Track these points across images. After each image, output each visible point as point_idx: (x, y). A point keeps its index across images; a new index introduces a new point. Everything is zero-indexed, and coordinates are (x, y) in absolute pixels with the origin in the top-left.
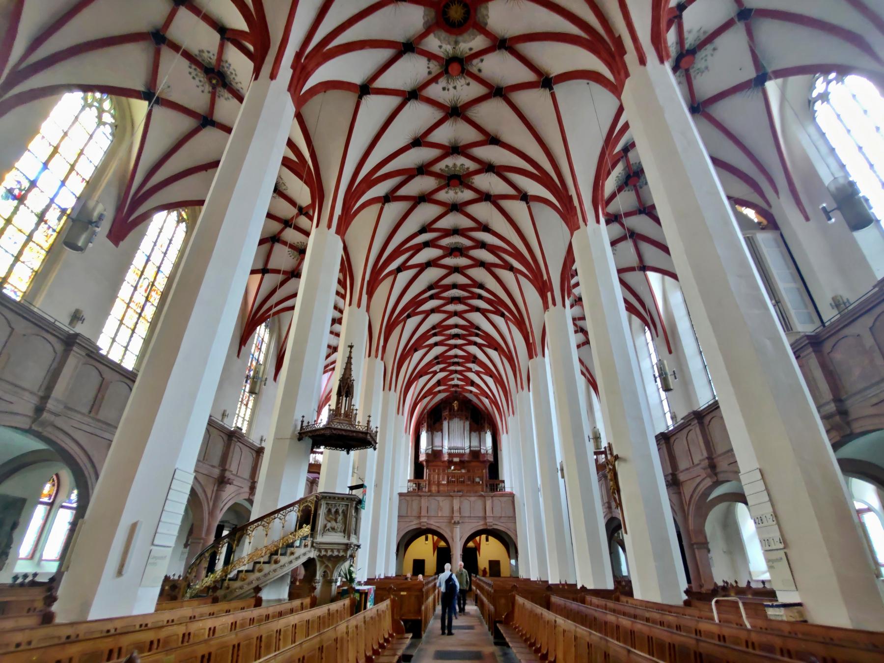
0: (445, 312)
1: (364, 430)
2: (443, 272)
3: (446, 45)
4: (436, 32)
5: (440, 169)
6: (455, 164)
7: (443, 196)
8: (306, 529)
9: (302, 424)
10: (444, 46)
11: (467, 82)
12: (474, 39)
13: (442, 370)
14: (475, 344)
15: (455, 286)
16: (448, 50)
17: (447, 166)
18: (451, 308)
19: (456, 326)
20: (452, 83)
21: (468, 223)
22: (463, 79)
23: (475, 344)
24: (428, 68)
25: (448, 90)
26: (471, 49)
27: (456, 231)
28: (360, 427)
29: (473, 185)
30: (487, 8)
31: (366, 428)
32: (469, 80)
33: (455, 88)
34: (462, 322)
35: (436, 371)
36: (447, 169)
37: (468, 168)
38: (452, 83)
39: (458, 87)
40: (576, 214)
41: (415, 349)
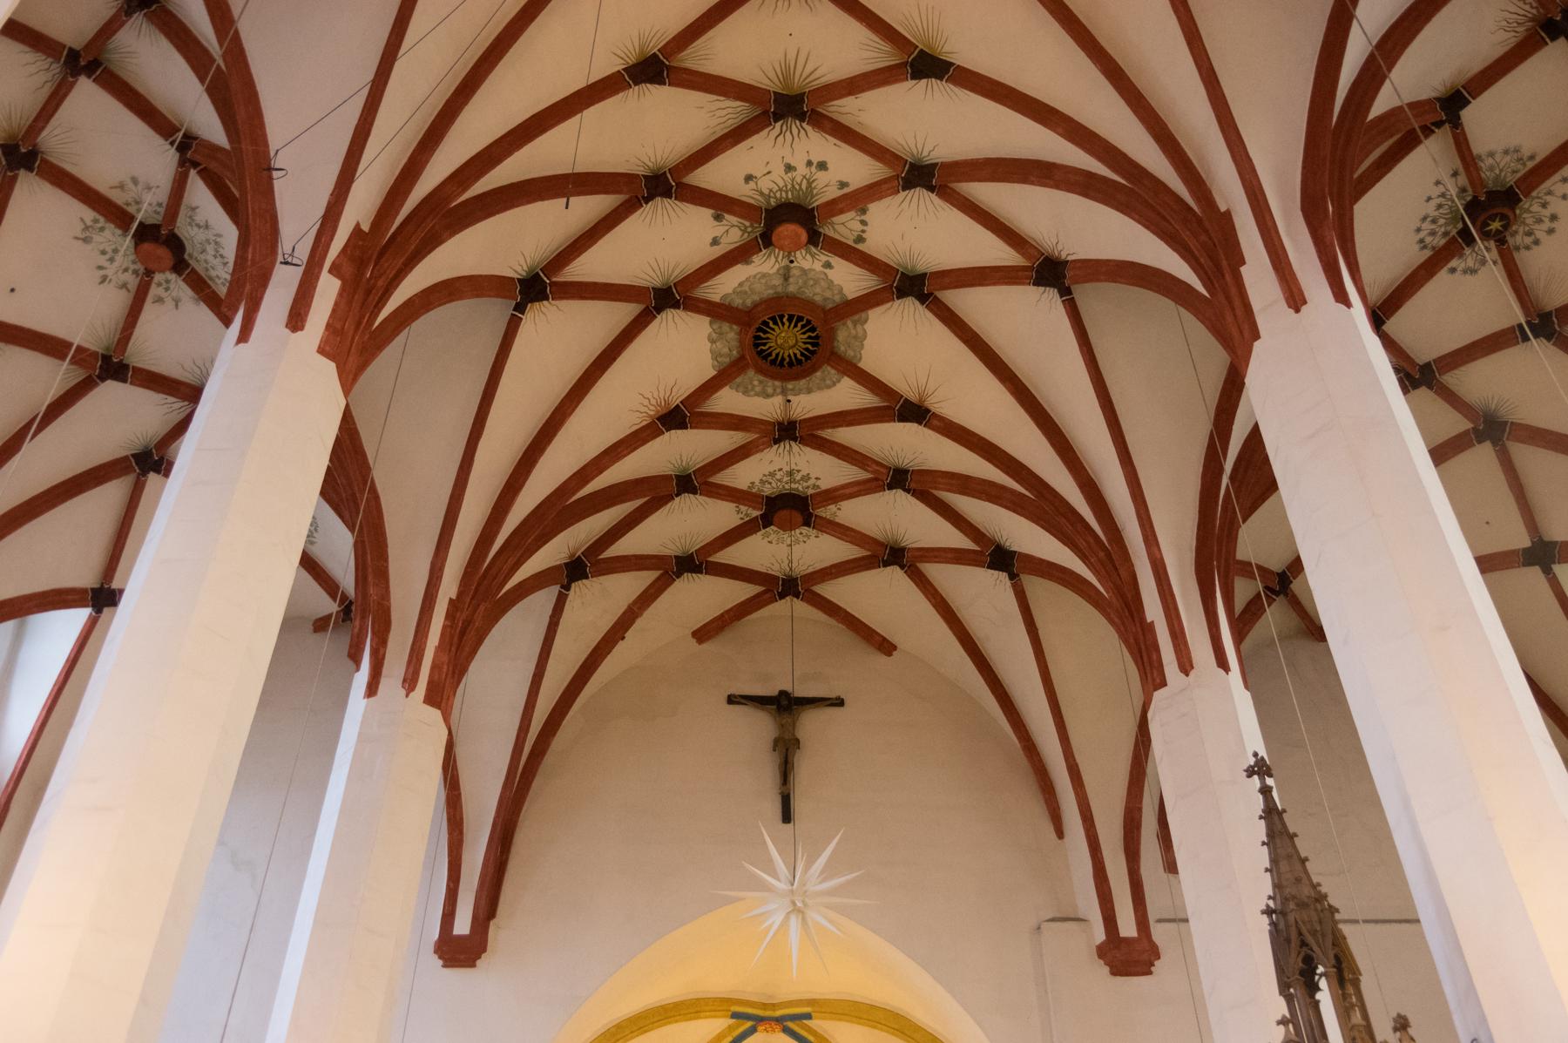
4: (837, 298)
10: (818, 266)
11: (752, 184)
12: (741, 285)
16: (808, 257)
20: (798, 179)
22: (767, 192)
24: (864, 223)
25: (809, 163)
30: (715, 355)
33: (789, 168)
38: (798, 179)
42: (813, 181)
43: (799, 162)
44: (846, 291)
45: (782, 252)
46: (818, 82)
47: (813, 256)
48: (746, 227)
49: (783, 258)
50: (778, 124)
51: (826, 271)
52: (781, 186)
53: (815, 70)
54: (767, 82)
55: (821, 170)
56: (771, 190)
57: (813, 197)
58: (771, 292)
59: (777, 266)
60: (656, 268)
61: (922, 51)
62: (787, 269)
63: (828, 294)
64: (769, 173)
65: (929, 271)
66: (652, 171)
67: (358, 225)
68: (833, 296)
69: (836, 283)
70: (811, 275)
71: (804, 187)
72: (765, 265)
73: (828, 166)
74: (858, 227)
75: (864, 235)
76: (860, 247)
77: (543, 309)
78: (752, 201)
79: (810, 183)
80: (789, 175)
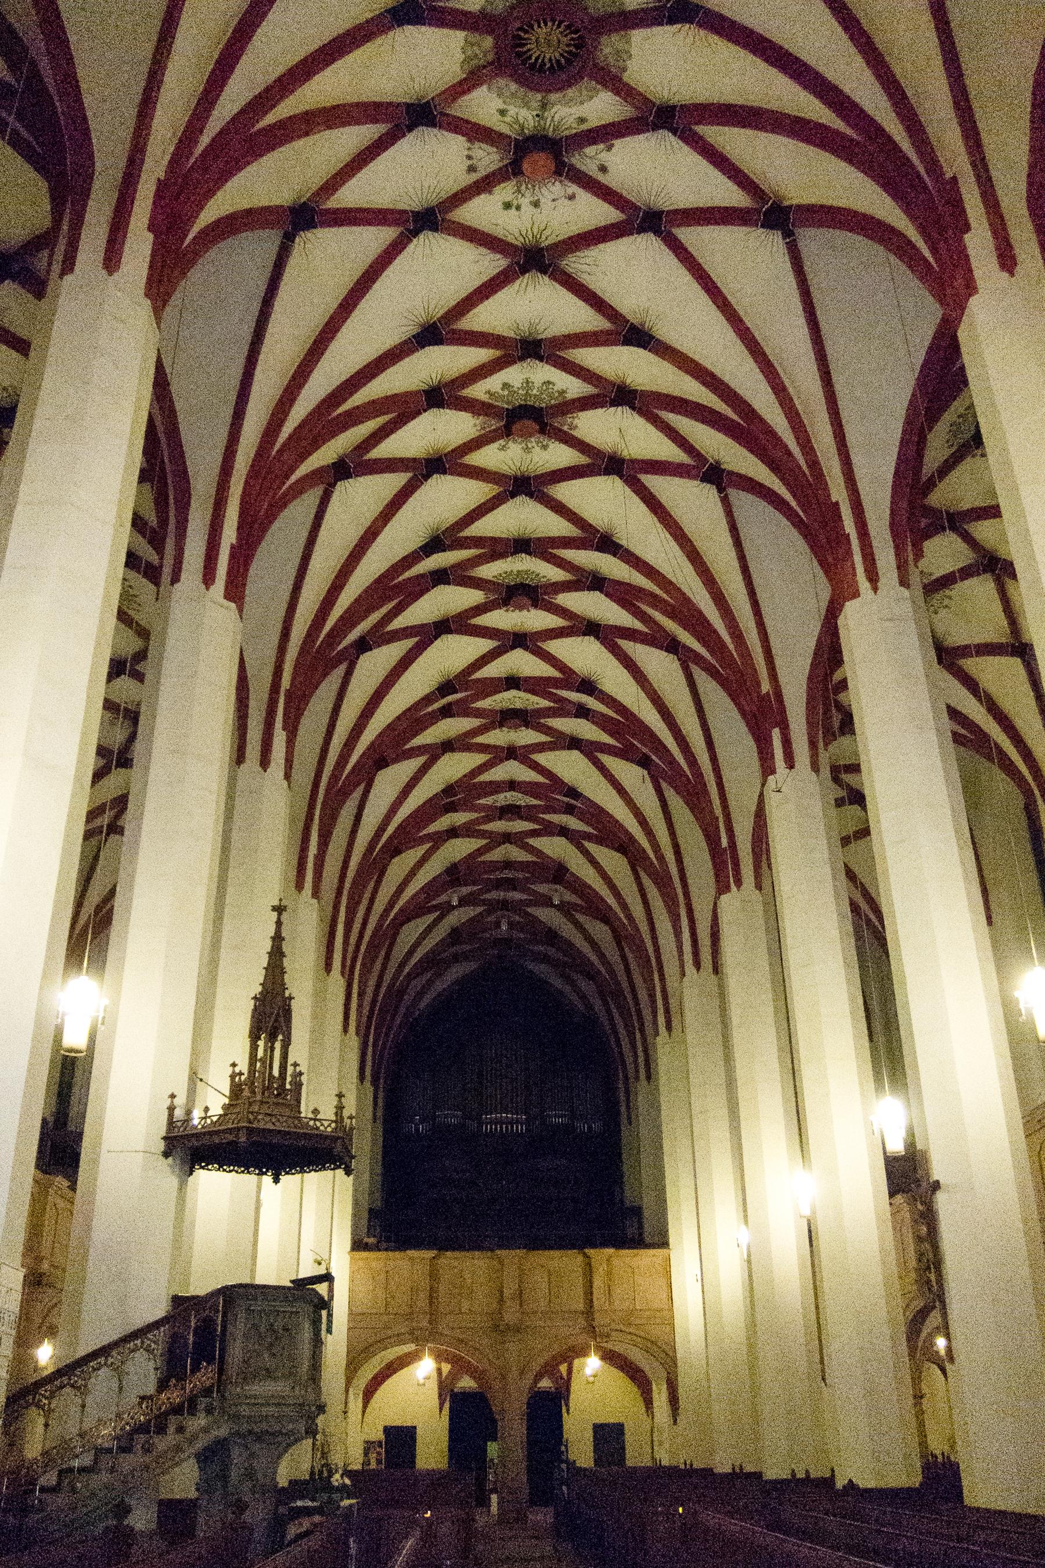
0: (483, 748)
1: (329, 1129)
2: (484, 645)
5: (488, 392)
7: (489, 457)
8: (206, 1376)
9: (171, 1115)
10: (512, 111)
12: (591, 98)
13: (463, 902)
14: (563, 831)
15: (512, 682)
17: (506, 386)
18: (498, 737)
19: (512, 785)
21: (558, 526)
23: (563, 831)
24: (469, 157)
25: (518, 208)
26: (582, 120)
27: (522, 545)
28: (318, 1124)
29: (575, 433)
31: (333, 1125)
32: (573, 188)
33: (536, 204)
34: (530, 776)
35: (449, 903)
38: (528, 194)
40: (849, 553)
41: (394, 849)
43: (527, 209)
64: (554, 200)
71: (523, 187)
79: (519, 191)
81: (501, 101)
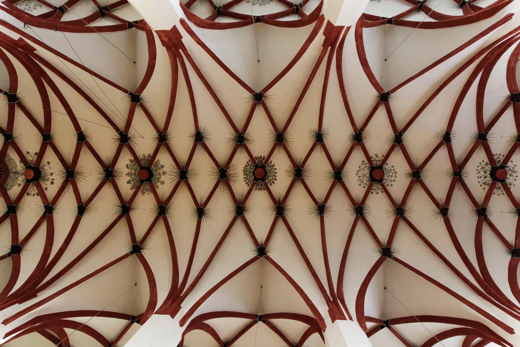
3: (18, 181)
4: (7, 188)
6: (128, 174)
10: (19, 182)
11: (47, 164)
12: (13, 160)
16: (22, 179)
17: (129, 182)
20: (48, 177)
22: (44, 168)
24: (34, 195)
25: (53, 180)
33: (52, 174)
36: (132, 182)
37: (131, 161)
38: (48, 177)
39: (51, 171)
42: (48, 181)
43: (53, 177)
44: (10, 190)
45: (24, 172)
46: (77, 182)
47: (22, 181)
48: (33, 162)
49: (22, 172)
50: (65, 171)
51: (18, 184)
52: (46, 172)
53: (81, 181)
54: (78, 168)
55: (51, 183)
56: (45, 169)
57: (42, 181)
58: (10, 168)
59: (19, 170)
60: (19, 135)
61: (86, 208)
62: (18, 173)
63: (9, 185)
64: (50, 168)
65: (17, 214)
66: (51, 136)
67: (36, 50)
68: (9, 187)
69: (13, 187)
70: (16, 180)
72: (20, 167)
73: (52, 185)
74: (33, 193)
75: (29, 195)
76: (26, 194)
77: (5, 100)
78: (41, 164)
79: (47, 180)
80: (50, 174)
81: (15, 186)
